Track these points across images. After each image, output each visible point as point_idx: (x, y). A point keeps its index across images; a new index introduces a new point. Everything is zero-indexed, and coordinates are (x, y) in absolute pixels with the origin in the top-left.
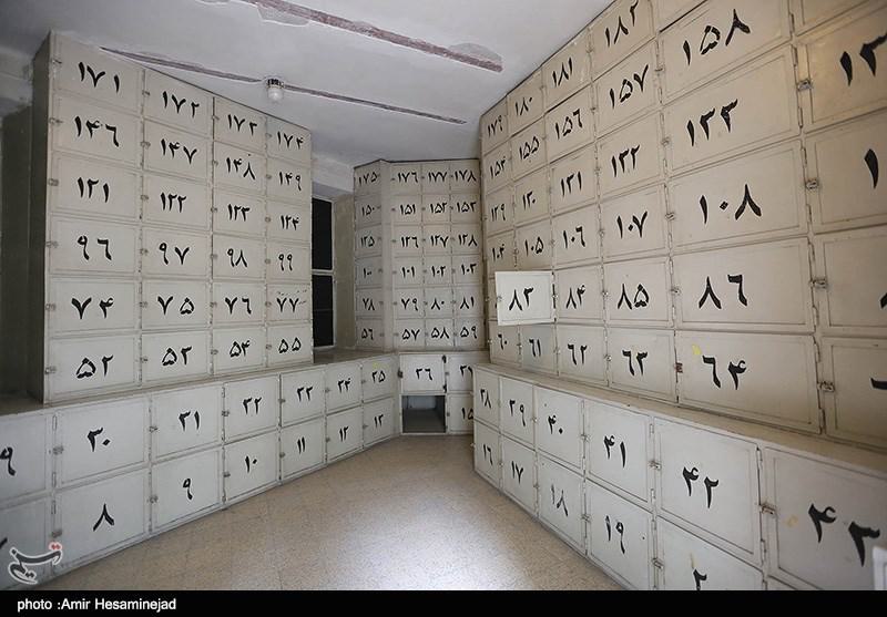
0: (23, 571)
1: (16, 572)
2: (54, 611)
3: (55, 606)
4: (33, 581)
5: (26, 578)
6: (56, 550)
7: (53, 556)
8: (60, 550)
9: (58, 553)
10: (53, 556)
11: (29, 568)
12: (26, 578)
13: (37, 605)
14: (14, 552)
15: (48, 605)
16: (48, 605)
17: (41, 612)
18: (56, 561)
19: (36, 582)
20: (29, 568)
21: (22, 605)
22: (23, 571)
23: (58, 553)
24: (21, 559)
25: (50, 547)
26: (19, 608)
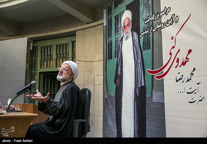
0: (5, 133)
1: (3, 133)
2: (11, 143)
3: (11, 141)
4: (7, 136)
5: (6, 135)
6: (13, 128)
7: (12, 130)
8: (14, 128)
9: (13, 129)
10: (12, 130)
11: (7, 133)
12: (6, 135)
13: (7, 141)
14: (3, 129)
15: (10, 141)
16: (10, 141)
17: (8, 143)
18: (13, 131)
19: (8, 136)
20: (7, 133)
21: (4, 141)
22: (5, 133)
23: (13, 129)
24: (5, 130)
25: (11, 128)
26: (3, 142)
